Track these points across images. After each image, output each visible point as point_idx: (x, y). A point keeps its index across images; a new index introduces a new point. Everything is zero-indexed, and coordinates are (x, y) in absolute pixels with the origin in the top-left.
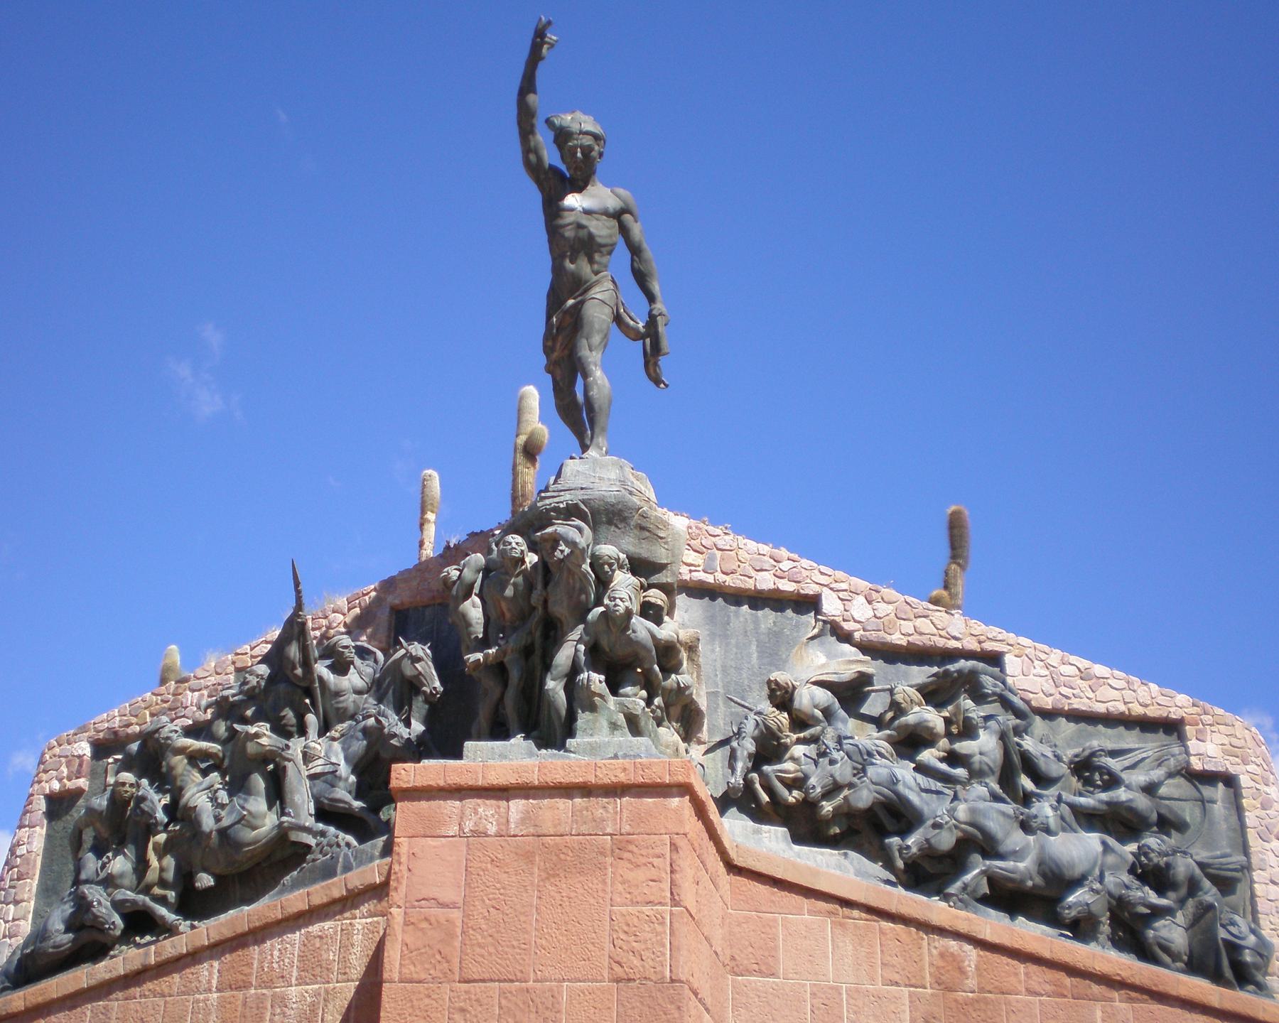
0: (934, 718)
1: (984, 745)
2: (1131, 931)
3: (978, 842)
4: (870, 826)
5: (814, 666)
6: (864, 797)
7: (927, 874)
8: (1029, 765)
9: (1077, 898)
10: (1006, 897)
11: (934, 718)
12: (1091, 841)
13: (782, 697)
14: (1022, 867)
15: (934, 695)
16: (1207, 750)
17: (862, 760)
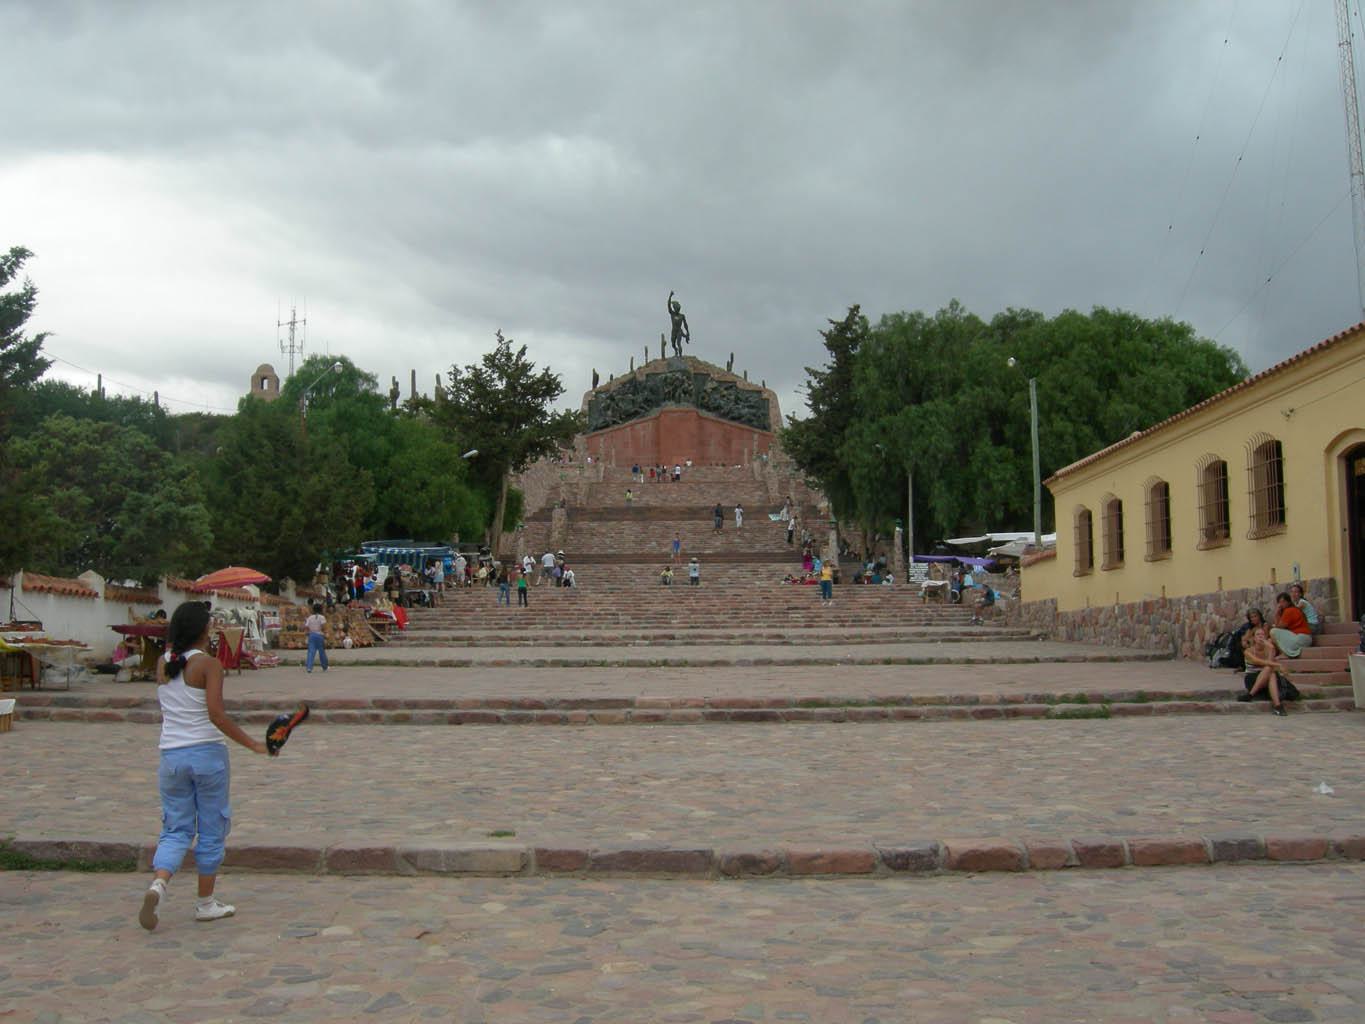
0: (725, 392)
1: (733, 397)
2: (749, 422)
3: (730, 411)
4: (717, 409)
5: (709, 386)
6: (716, 405)
7: (724, 415)
8: (739, 398)
9: (743, 419)
10: (733, 419)
11: (725, 392)
12: (746, 410)
13: (705, 391)
14: (736, 414)
15: (726, 389)
16: (765, 396)
17: (716, 400)
